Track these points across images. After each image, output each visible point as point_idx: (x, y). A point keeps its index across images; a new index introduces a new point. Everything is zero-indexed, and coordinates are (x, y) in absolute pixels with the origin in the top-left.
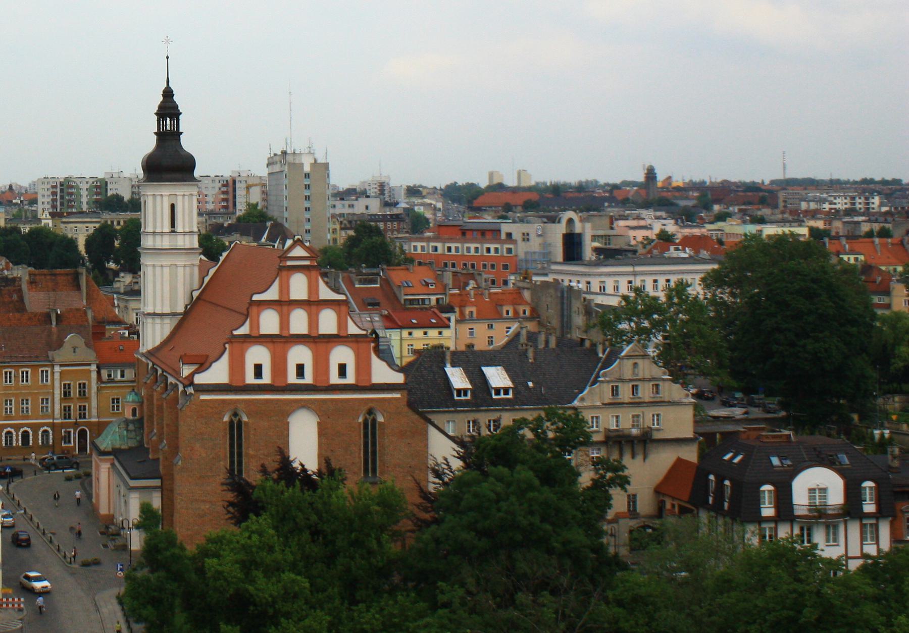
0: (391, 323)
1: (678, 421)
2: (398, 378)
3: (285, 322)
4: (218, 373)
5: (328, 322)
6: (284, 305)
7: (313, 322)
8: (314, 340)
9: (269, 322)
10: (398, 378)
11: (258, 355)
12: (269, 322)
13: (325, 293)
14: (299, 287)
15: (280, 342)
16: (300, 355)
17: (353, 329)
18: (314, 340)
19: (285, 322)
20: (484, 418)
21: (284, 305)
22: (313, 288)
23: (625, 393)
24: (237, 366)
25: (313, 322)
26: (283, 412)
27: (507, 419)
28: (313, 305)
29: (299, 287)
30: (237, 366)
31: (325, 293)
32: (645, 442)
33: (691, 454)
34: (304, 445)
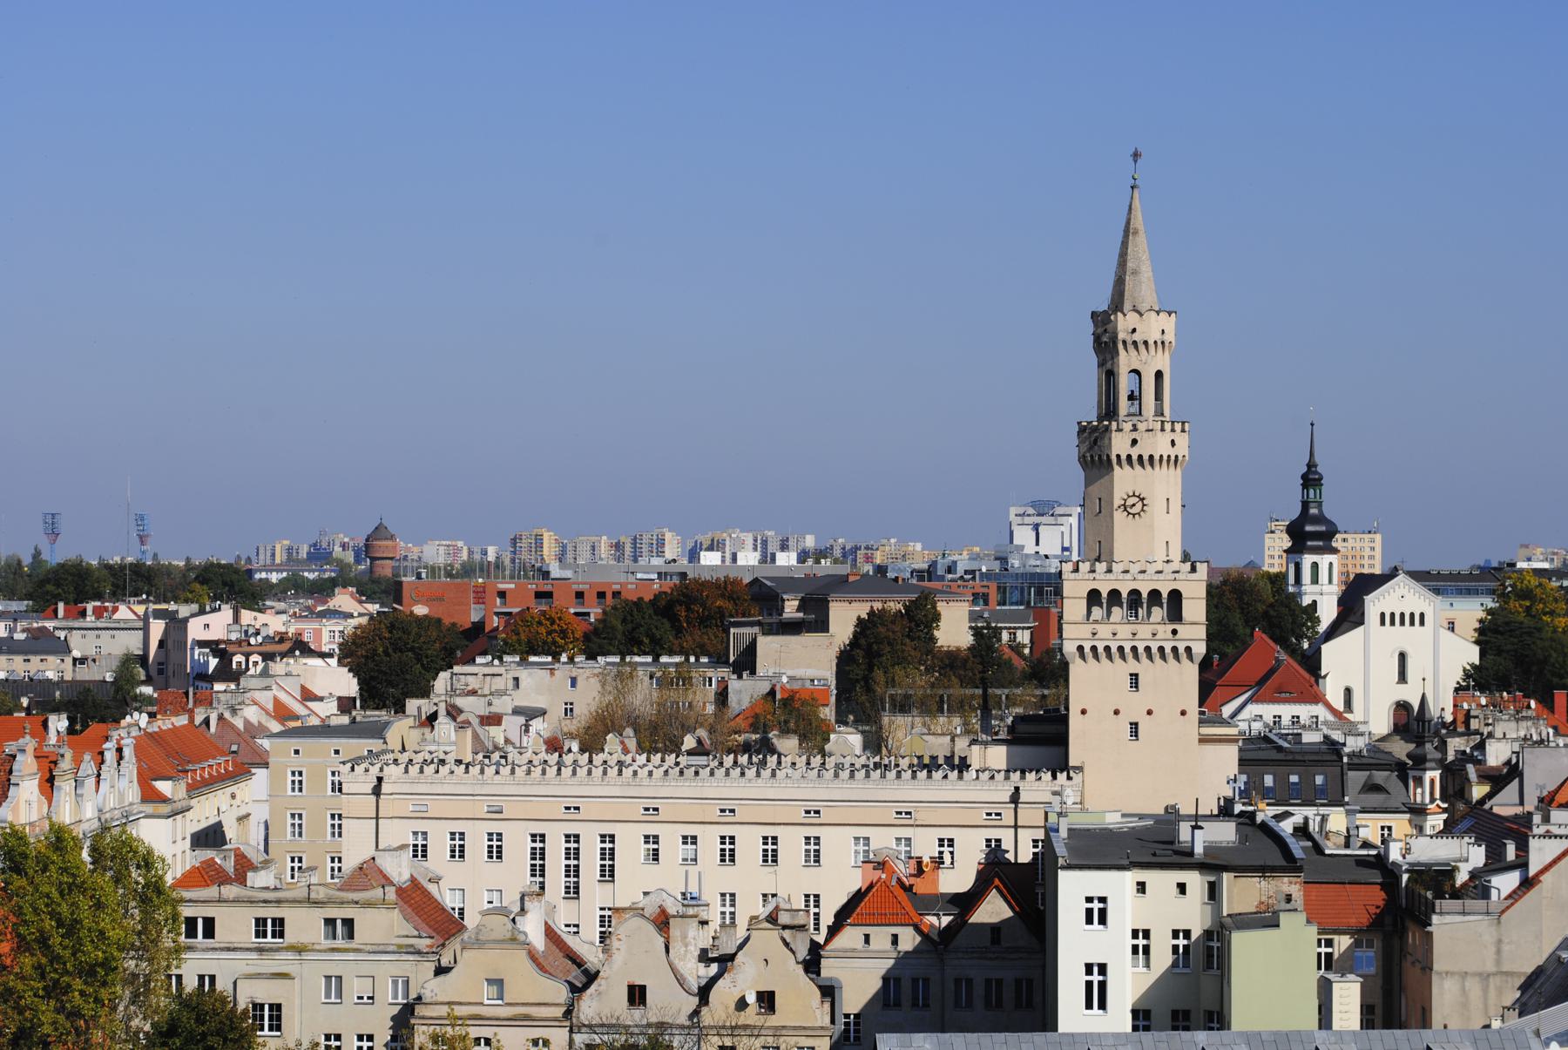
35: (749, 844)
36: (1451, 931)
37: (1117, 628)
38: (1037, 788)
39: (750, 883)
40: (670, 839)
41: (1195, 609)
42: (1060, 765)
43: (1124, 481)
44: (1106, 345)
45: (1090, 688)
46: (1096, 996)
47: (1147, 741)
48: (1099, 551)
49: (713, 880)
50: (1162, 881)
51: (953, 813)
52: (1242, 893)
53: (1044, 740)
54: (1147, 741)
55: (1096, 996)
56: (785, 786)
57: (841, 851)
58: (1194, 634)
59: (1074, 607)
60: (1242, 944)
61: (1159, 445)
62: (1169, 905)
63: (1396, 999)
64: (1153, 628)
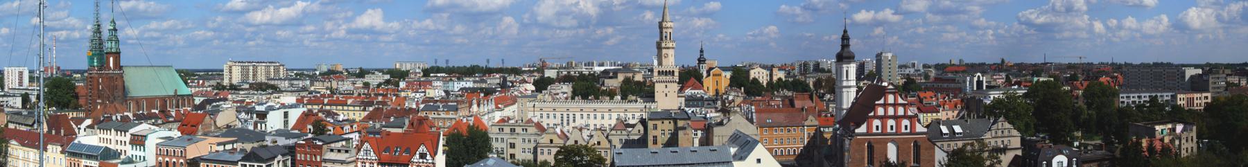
0: (920, 110)
1: (1016, 142)
2: (925, 130)
3: (886, 111)
4: (863, 129)
5: (901, 111)
6: (885, 105)
7: (895, 111)
8: (895, 117)
9: (881, 111)
10: (925, 130)
11: (877, 122)
12: (881, 111)
13: (900, 101)
14: (891, 99)
15: (884, 118)
16: (891, 122)
17: (910, 113)
18: (895, 117)
19: (886, 111)
20: (952, 143)
21: (885, 105)
22: (895, 99)
23: (1000, 133)
24: (869, 127)
25: (895, 111)
26: (885, 142)
27: (960, 144)
28: (895, 105)
29: (891, 99)
30: (869, 127)
31: (900, 101)
32: (1004, 150)
33: (1019, 153)
34: (892, 153)
35: (599, 115)
36: (717, 131)
37: (663, 78)
38: (648, 105)
39: (599, 122)
40: (585, 115)
41: (677, 74)
42: (653, 101)
43: (664, 51)
44: (661, 27)
45: (659, 88)
46: (655, 142)
47: (668, 98)
48: (660, 64)
49: (592, 122)
50: (666, 122)
51: (634, 110)
52: (680, 123)
53: (649, 96)
54: (668, 98)
55: (655, 142)
56: (605, 104)
57: (615, 116)
58: (676, 78)
59: (656, 74)
60: (681, 133)
61: (670, 45)
62: (668, 126)
63: (706, 141)
64: (669, 78)
